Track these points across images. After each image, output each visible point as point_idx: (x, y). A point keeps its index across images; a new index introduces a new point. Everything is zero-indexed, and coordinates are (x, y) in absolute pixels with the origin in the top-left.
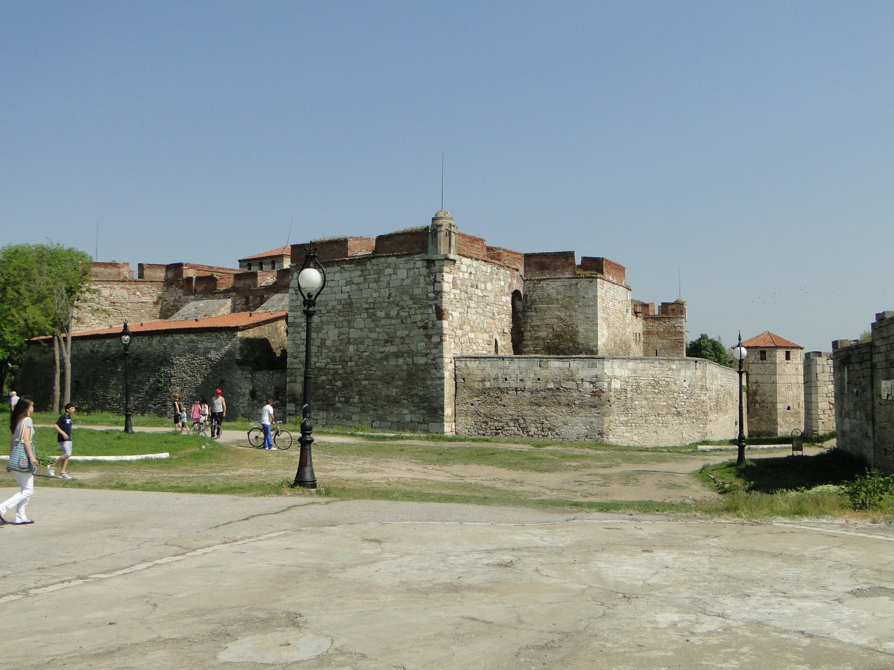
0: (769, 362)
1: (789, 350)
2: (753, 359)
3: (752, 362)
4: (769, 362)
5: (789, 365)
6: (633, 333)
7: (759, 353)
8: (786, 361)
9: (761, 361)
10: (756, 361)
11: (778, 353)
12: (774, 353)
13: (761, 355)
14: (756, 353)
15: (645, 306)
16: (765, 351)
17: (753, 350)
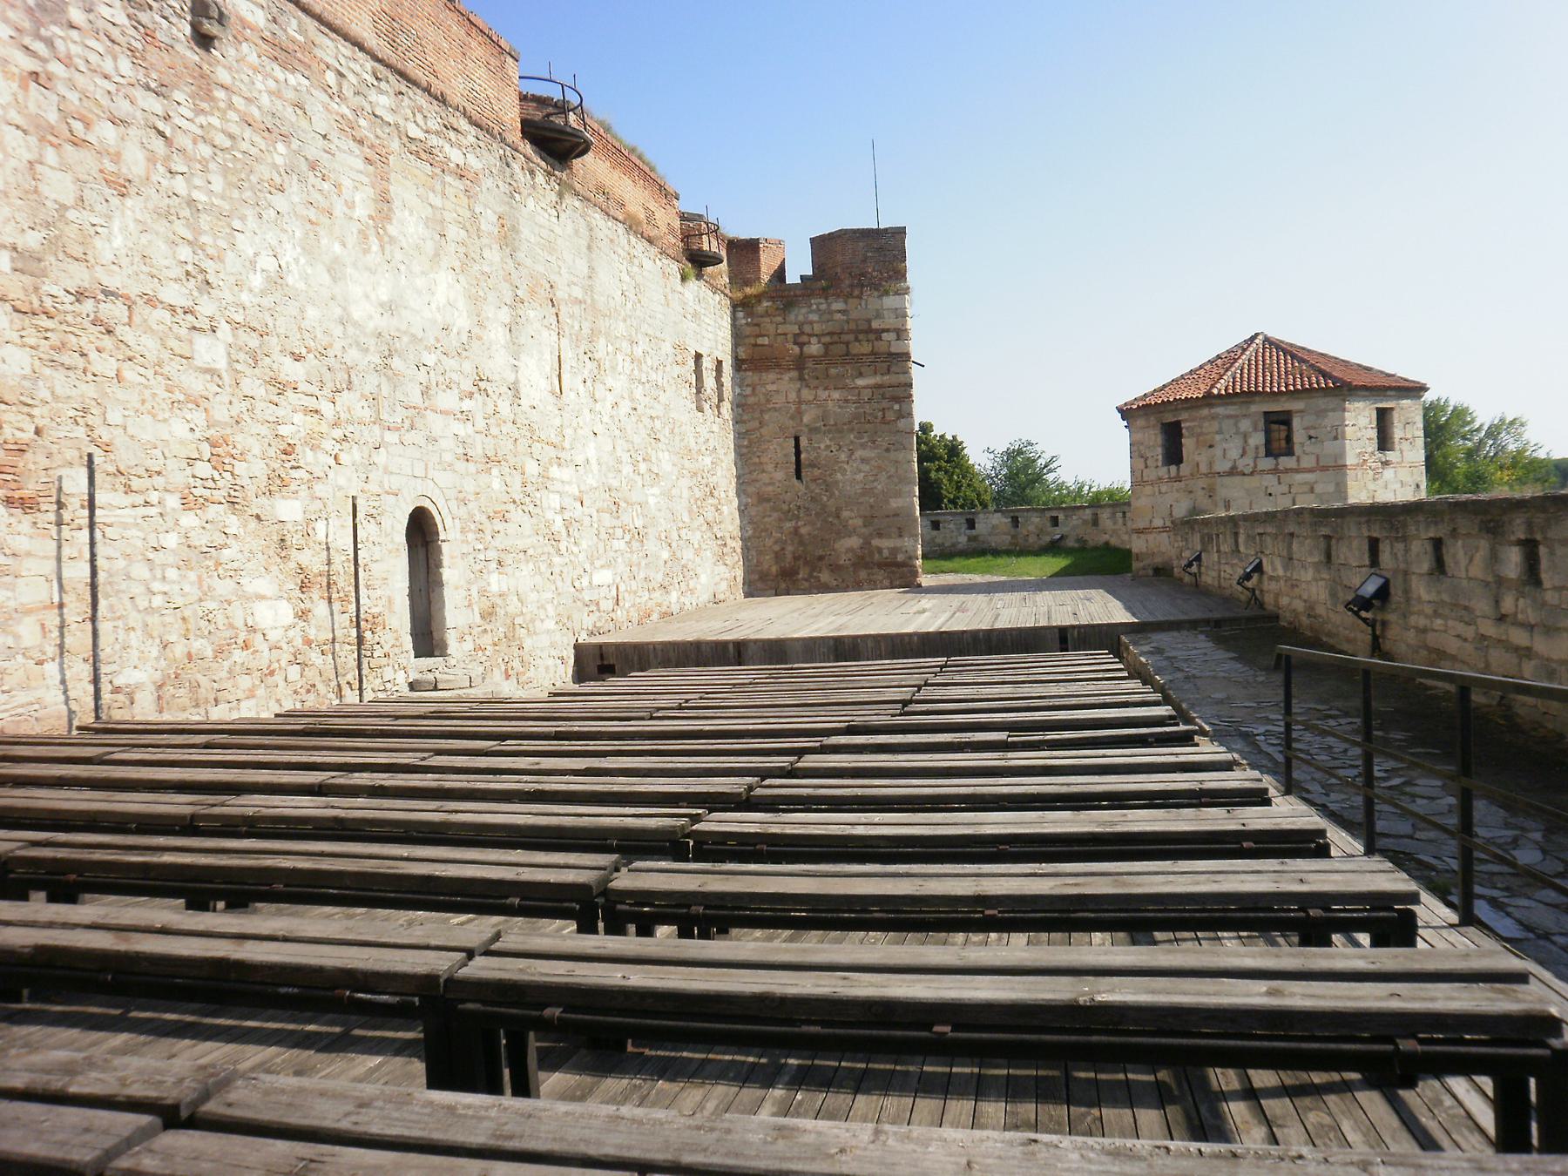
0: (1308, 462)
1: (1414, 390)
2: (1234, 453)
3: (1226, 466)
4: (1308, 462)
5: (1388, 473)
6: (680, 348)
7: (1261, 424)
8: (1379, 455)
9: (1268, 463)
10: (1246, 464)
11: (1349, 418)
12: (1330, 419)
13: (1267, 432)
14: (1245, 425)
15: (745, 251)
16: (1289, 413)
17: (1231, 410)
